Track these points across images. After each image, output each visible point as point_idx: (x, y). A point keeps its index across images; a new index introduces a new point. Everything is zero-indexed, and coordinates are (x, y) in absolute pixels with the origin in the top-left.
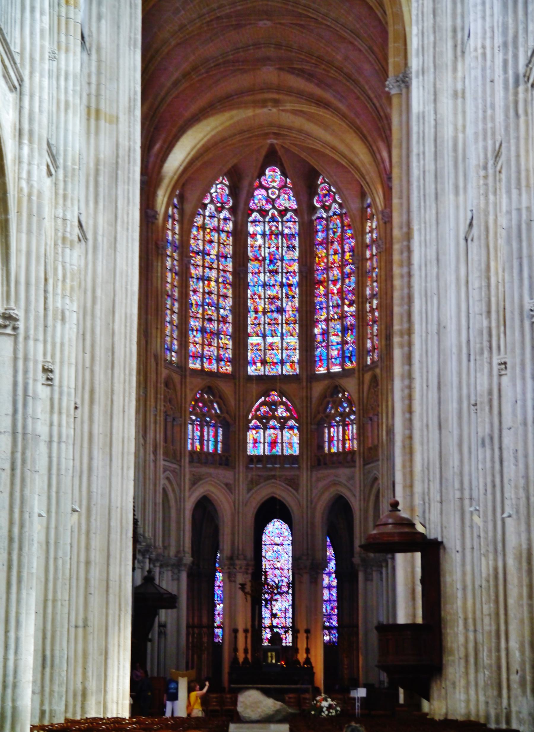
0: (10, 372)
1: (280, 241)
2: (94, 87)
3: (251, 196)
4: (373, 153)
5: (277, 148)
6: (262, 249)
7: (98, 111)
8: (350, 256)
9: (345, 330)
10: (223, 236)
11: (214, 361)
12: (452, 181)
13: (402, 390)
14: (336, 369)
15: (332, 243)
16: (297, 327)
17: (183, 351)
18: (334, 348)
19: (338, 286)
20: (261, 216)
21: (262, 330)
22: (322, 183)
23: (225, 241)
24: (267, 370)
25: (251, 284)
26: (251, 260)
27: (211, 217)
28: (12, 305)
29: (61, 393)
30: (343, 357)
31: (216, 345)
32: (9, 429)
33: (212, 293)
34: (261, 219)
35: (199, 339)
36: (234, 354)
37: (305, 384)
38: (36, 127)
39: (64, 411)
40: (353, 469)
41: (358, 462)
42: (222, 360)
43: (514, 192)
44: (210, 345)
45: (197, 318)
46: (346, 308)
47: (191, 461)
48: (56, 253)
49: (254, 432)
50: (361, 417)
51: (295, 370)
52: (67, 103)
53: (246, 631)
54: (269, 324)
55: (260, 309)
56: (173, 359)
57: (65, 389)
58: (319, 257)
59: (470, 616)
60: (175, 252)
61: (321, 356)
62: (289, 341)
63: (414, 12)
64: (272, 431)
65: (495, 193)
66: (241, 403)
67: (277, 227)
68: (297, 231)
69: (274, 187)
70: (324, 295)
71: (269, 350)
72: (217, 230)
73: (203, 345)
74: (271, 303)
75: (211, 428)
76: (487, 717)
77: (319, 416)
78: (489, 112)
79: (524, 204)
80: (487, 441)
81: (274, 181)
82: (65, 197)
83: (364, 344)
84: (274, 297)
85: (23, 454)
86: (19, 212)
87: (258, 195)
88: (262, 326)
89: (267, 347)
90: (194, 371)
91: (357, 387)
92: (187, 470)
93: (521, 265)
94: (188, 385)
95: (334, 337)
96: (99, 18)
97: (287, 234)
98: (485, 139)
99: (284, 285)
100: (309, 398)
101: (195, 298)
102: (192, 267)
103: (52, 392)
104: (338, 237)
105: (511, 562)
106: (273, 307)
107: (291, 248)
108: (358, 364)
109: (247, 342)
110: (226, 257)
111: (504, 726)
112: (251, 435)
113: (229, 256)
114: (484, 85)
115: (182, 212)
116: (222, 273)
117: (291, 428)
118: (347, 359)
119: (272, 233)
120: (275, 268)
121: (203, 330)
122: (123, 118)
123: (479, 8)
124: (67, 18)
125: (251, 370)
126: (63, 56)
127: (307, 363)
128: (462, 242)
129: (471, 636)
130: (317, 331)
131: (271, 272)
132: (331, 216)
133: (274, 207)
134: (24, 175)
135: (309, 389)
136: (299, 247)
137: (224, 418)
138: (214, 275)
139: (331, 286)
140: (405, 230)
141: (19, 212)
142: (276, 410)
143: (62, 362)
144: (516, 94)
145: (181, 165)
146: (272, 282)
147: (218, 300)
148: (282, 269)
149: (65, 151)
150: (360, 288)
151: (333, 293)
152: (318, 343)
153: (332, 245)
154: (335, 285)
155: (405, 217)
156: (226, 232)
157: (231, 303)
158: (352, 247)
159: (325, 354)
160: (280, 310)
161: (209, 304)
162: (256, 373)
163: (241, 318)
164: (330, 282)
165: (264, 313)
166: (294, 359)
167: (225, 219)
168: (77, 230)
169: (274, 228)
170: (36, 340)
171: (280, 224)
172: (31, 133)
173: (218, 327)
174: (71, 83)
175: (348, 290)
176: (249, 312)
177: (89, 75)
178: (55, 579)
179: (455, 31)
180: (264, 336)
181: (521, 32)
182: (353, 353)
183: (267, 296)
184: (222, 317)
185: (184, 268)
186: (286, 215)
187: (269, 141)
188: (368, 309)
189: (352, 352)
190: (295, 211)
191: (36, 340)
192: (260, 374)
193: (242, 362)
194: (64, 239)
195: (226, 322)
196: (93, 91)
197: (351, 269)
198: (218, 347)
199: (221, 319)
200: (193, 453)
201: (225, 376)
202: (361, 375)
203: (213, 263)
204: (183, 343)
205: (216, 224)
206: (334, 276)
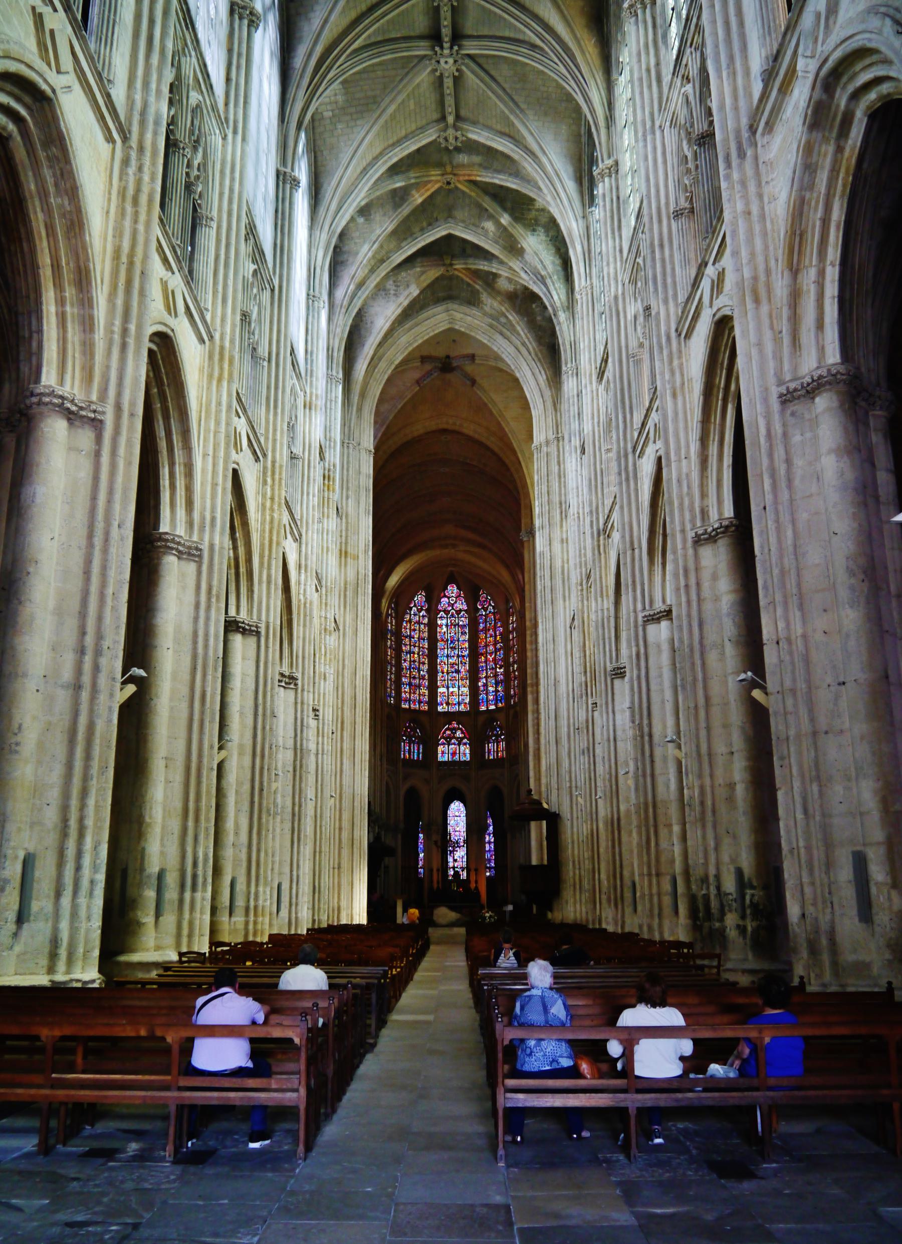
0: (293, 711)
2: (344, 538)
3: (440, 602)
4: (513, 576)
7: (346, 553)
9: (497, 683)
10: (422, 626)
12: (561, 593)
13: (533, 721)
14: (492, 707)
27: (415, 615)
28: (294, 670)
29: (323, 724)
30: (496, 700)
32: (292, 746)
35: (407, 689)
38: (309, 563)
39: (326, 735)
43: (599, 599)
44: (414, 693)
48: (321, 638)
52: (328, 548)
53: (438, 870)
55: (445, 670)
57: (326, 721)
59: (576, 859)
63: (536, 493)
65: (588, 600)
72: (419, 623)
73: (410, 693)
74: (452, 667)
76: (587, 920)
78: (583, 551)
79: (605, 607)
80: (586, 751)
82: (326, 604)
85: (301, 761)
86: (299, 614)
90: (405, 709)
93: (604, 643)
96: (347, 498)
98: (581, 567)
101: (405, 665)
103: (318, 723)
105: (601, 825)
107: (463, 633)
108: (506, 704)
111: (597, 926)
112: (440, 748)
114: (579, 535)
115: (396, 613)
117: (465, 744)
119: (452, 624)
121: (410, 684)
122: (361, 556)
123: (575, 490)
124: (328, 498)
125: (440, 709)
126: (326, 520)
128: (568, 629)
129: (577, 872)
130: (480, 684)
134: (302, 592)
140: (533, 622)
141: (299, 614)
143: (324, 705)
144: (599, 541)
149: (327, 576)
155: (533, 614)
160: (458, 672)
165: (448, 673)
167: (423, 616)
168: (333, 624)
170: (309, 692)
172: (306, 566)
174: (330, 536)
177: (341, 531)
178: (321, 839)
179: (561, 503)
180: (448, 688)
181: (600, 504)
187: (450, 569)
190: (466, 611)
191: (309, 692)
194: (325, 630)
196: (344, 541)
198: (419, 695)
201: (424, 712)
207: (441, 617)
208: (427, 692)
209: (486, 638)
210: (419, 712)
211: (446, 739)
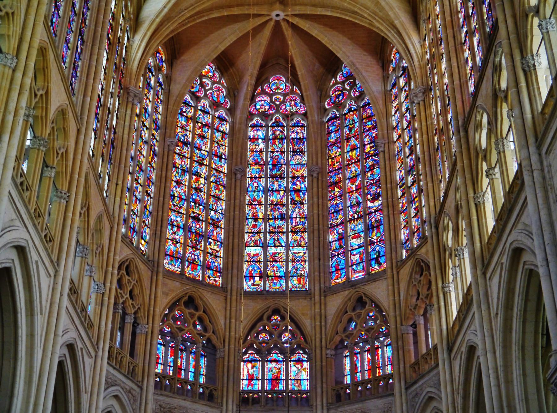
1: (285, 145)
5: (284, 25)
6: (264, 153)
8: (371, 147)
9: (369, 229)
10: (218, 135)
11: (199, 268)
15: (348, 140)
16: (306, 236)
17: (157, 242)
18: (355, 252)
19: (357, 183)
20: (262, 120)
21: (263, 239)
22: (334, 84)
23: (220, 141)
24: (268, 285)
25: (250, 189)
26: (251, 164)
27: (205, 112)
30: (367, 261)
31: (202, 249)
33: (201, 191)
34: (264, 123)
35: (180, 235)
36: (226, 264)
37: (317, 298)
40: (390, 398)
41: (398, 386)
42: (209, 268)
44: (195, 247)
45: (179, 213)
46: (369, 204)
47: (158, 386)
49: (250, 365)
50: (398, 326)
51: (304, 285)
54: (270, 232)
55: (261, 215)
56: (143, 249)
58: (332, 158)
60: (156, 130)
61: (338, 265)
62: (296, 251)
64: (274, 364)
66: (233, 321)
67: (281, 132)
68: (305, 136)
69: (278, 93)
70: (340, 196)
71: (270, 261)
73: (185, 245)
75: (192, 356)
77: (337, 339)
81: (277, 88)
83: (397, 236)
84: (277, 204)
87: (259, 101)
88: (262, 235)
89: (268, 258)
91: (390, 287)
92: (151, 396)
94: (160, 283)
95: (354, 240)
97: (293, 138)
99: (291, 191)
100: (323, 317)
102: (176, 156)
104: (355, 132)
106: (276, 214)
109: (243, 252)
110: (220, 158)
112: (245, 369)
113: (223, 157)
115: (168, 94)
116: (214, 172)
117: (299, 361)
118: (373, 262)
119: (275, 138)
120: (279, 173)
121: (187, 229)
125: (247, 285)
127: (320, 273)
130: (331, 238)
131: (273, 177)
132: (346, 114)
133: (277, 111)
135: (323, 304)
136: (308, 151)
137: (209, 340)
138: (204, 171)
139: (349, 184)
142: (280, 335)
145: (165, 7)
146: (276, 186)
147: (208, 200)
148: (288, 174)
150: (388, 173)
151: (352, 192)
152: (334, 250)
153: (348, 142)
154: (353, 183)
156: (221, 132)
157: (224, 207)
158: (374, 137)
159: (343, 261)
161: (195, 201)
162: (253, 289)
163: (237, 222)
164: (347, 181)
166: (303, 272)
169: (278, 133)
171: (285, 129)
173: (206, 229)
175: (371, 184)
176: (247, 219)
180: (265, 247)
182: (382, 253)
183: (269, 202)
184: (213, 220)
185: (166, 150)
186: (292, 120)
187: (274, 14)
188: (399, 192)
189: (379, 252)
192: (259, 290)
193: (235, 271)
195: (218, 227)
197: (374, 160)
198: (206, 253)
199: (210, 221)
200: (163, 376)
201: (213, 287)
202: (395, 272)
203: (203, 159)
204: (158, 233)
205: (210, 121)
206: (351, 172)
207: (254, 126)
208: (221, 253)
209: (342, 155)
210: (202, 284)
211: (258, 352)
